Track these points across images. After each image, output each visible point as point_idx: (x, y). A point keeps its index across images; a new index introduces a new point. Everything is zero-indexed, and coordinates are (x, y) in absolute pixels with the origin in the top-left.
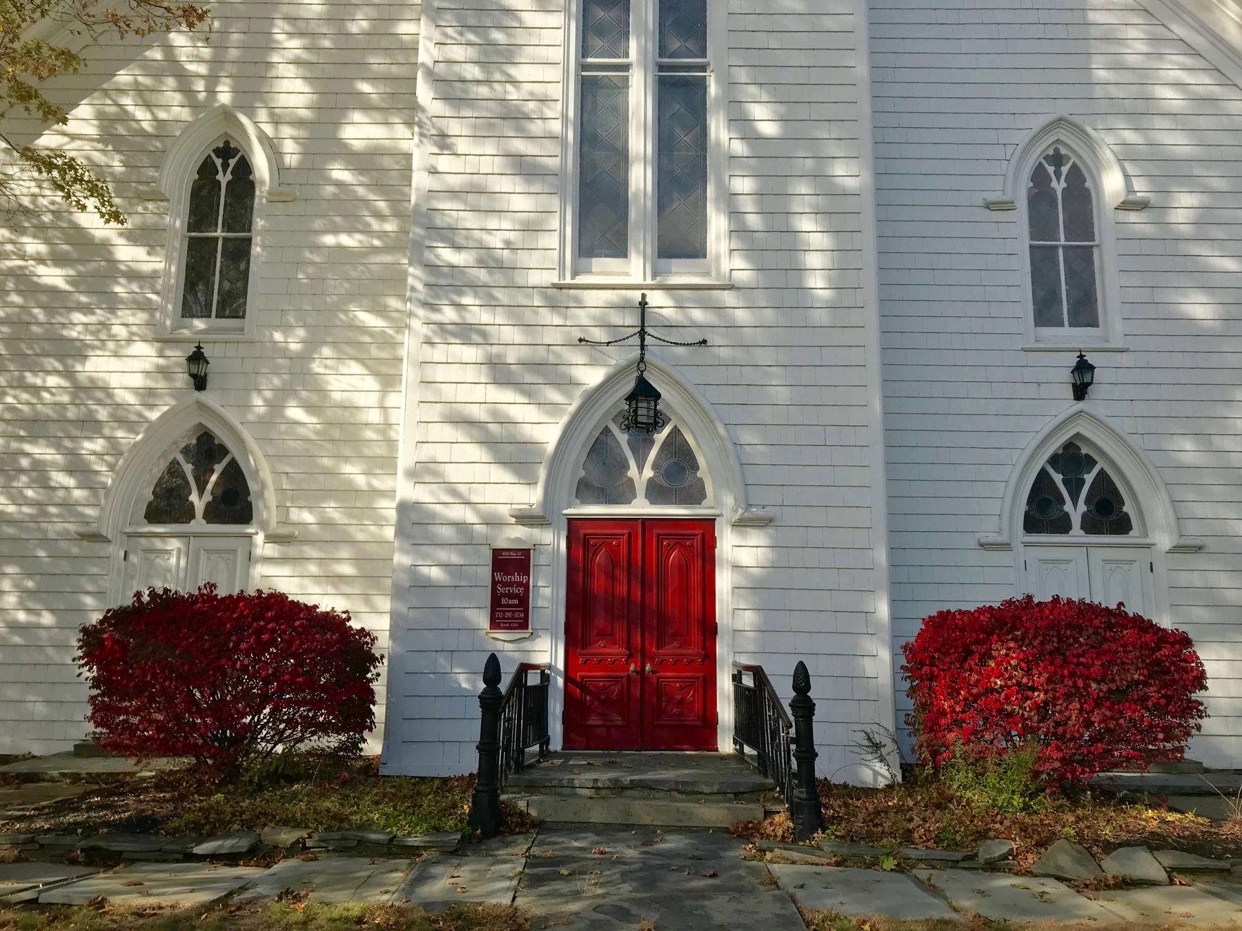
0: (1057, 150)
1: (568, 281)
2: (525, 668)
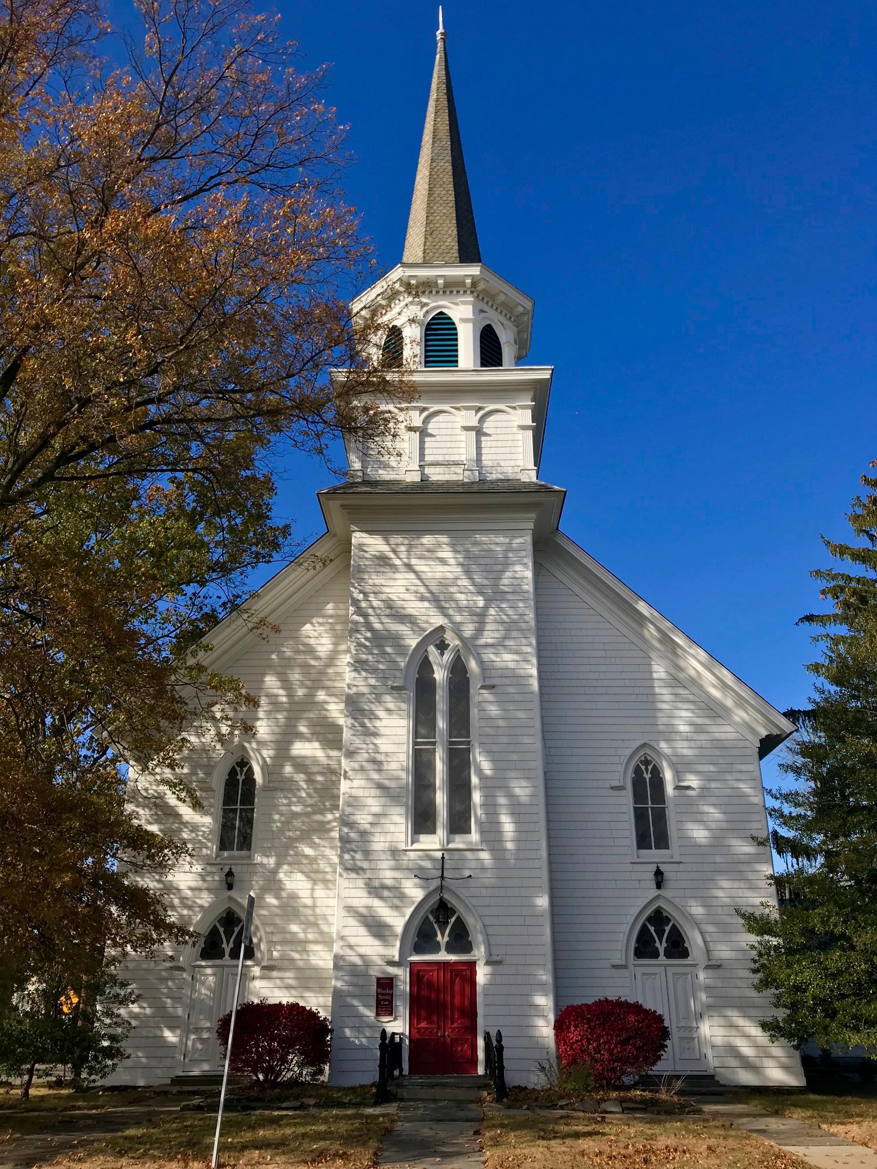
0: (646, 758)
1: (409, 848)
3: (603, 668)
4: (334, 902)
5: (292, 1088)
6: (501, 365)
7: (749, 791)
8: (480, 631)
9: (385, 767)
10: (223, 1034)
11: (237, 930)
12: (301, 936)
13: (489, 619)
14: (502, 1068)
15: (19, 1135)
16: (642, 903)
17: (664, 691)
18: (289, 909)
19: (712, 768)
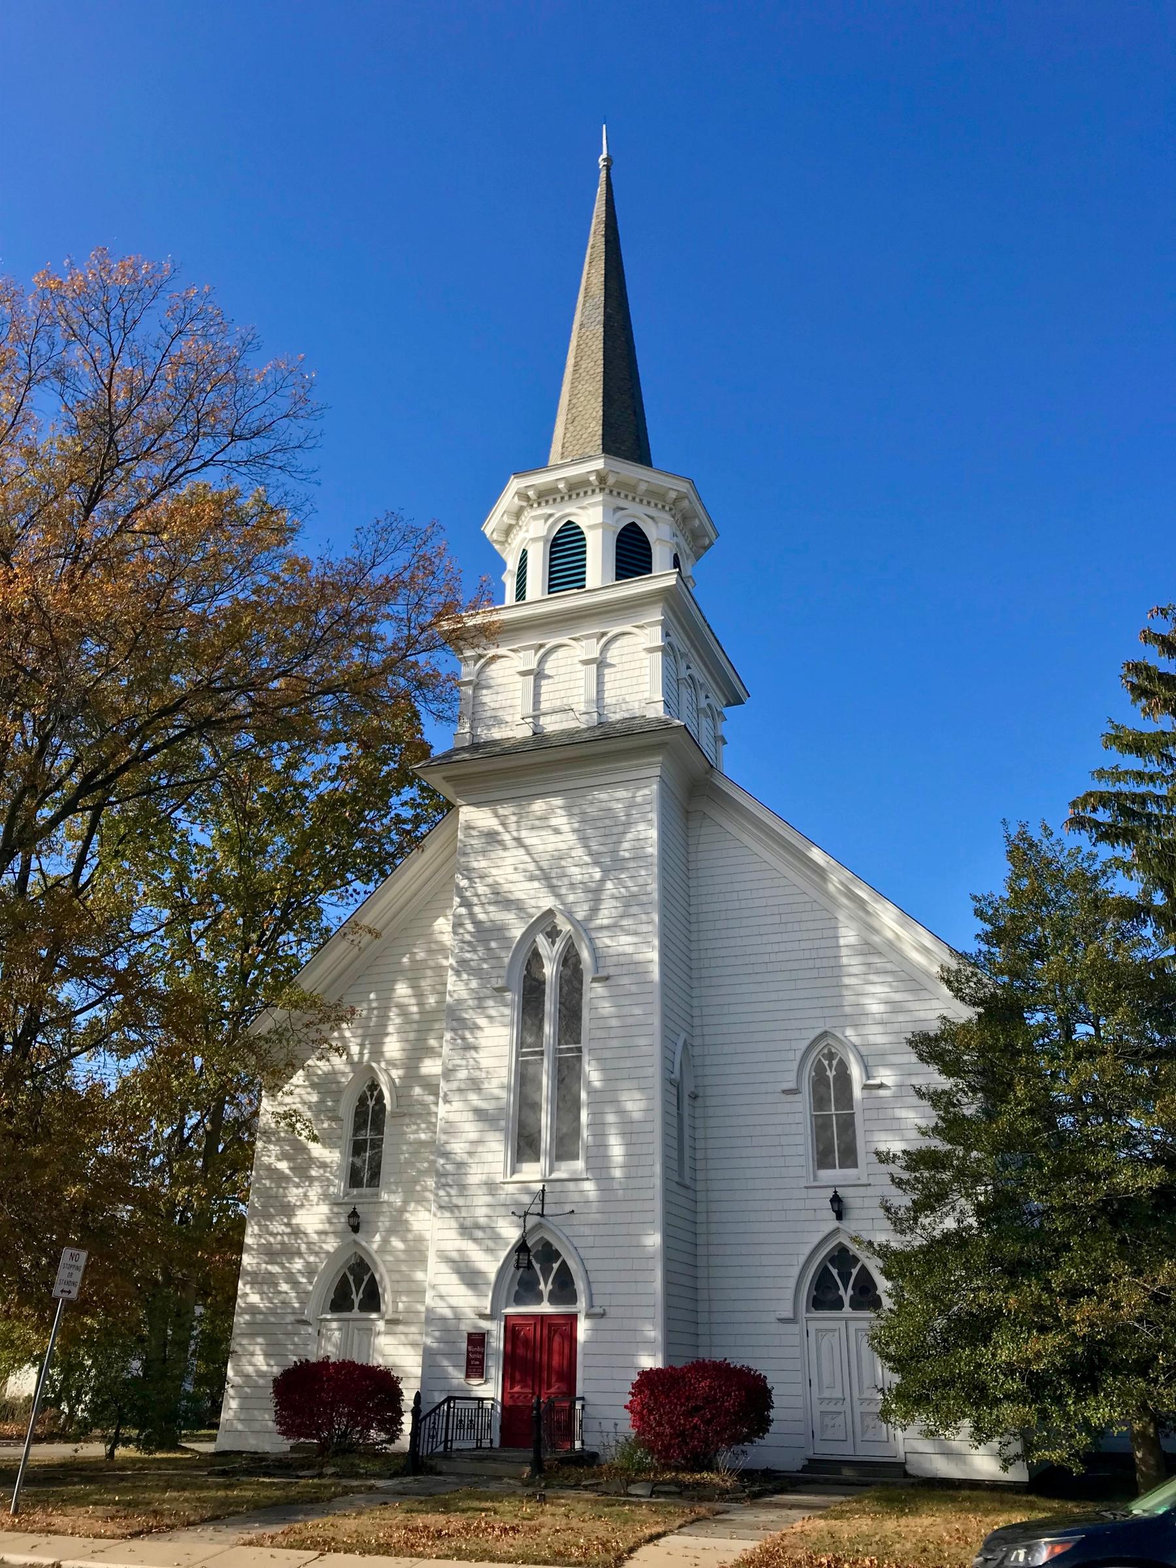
1: (509, 1180)
3: (778, 938)
6: (650, 572)
8: (594, 910)
9: (486, 1086)
13: (605, 895)
16: (816, 1239)
17: (855, 960)
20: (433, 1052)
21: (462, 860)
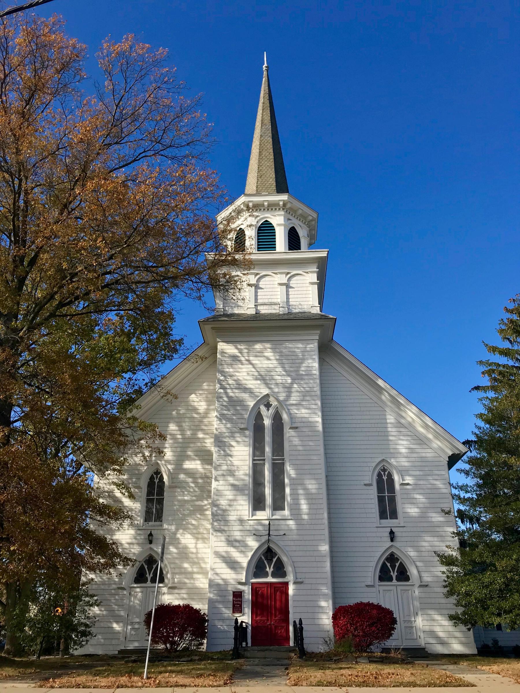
0: (384, 467)
1: (251, 518)
2: (242, 622)
4: (208, 551)
5: (186, 651)
7: (441, 486)
8: (288, 397)
9: (237, 474)
10: (148, 623)
11: (154, 566)
12: (190, 570)
13: (293, 390)
14: (302, 639)
15: (39, 670)
18: (183, 554)
19: (421, 473)
20: (191, 458)
21: (220, 367)
